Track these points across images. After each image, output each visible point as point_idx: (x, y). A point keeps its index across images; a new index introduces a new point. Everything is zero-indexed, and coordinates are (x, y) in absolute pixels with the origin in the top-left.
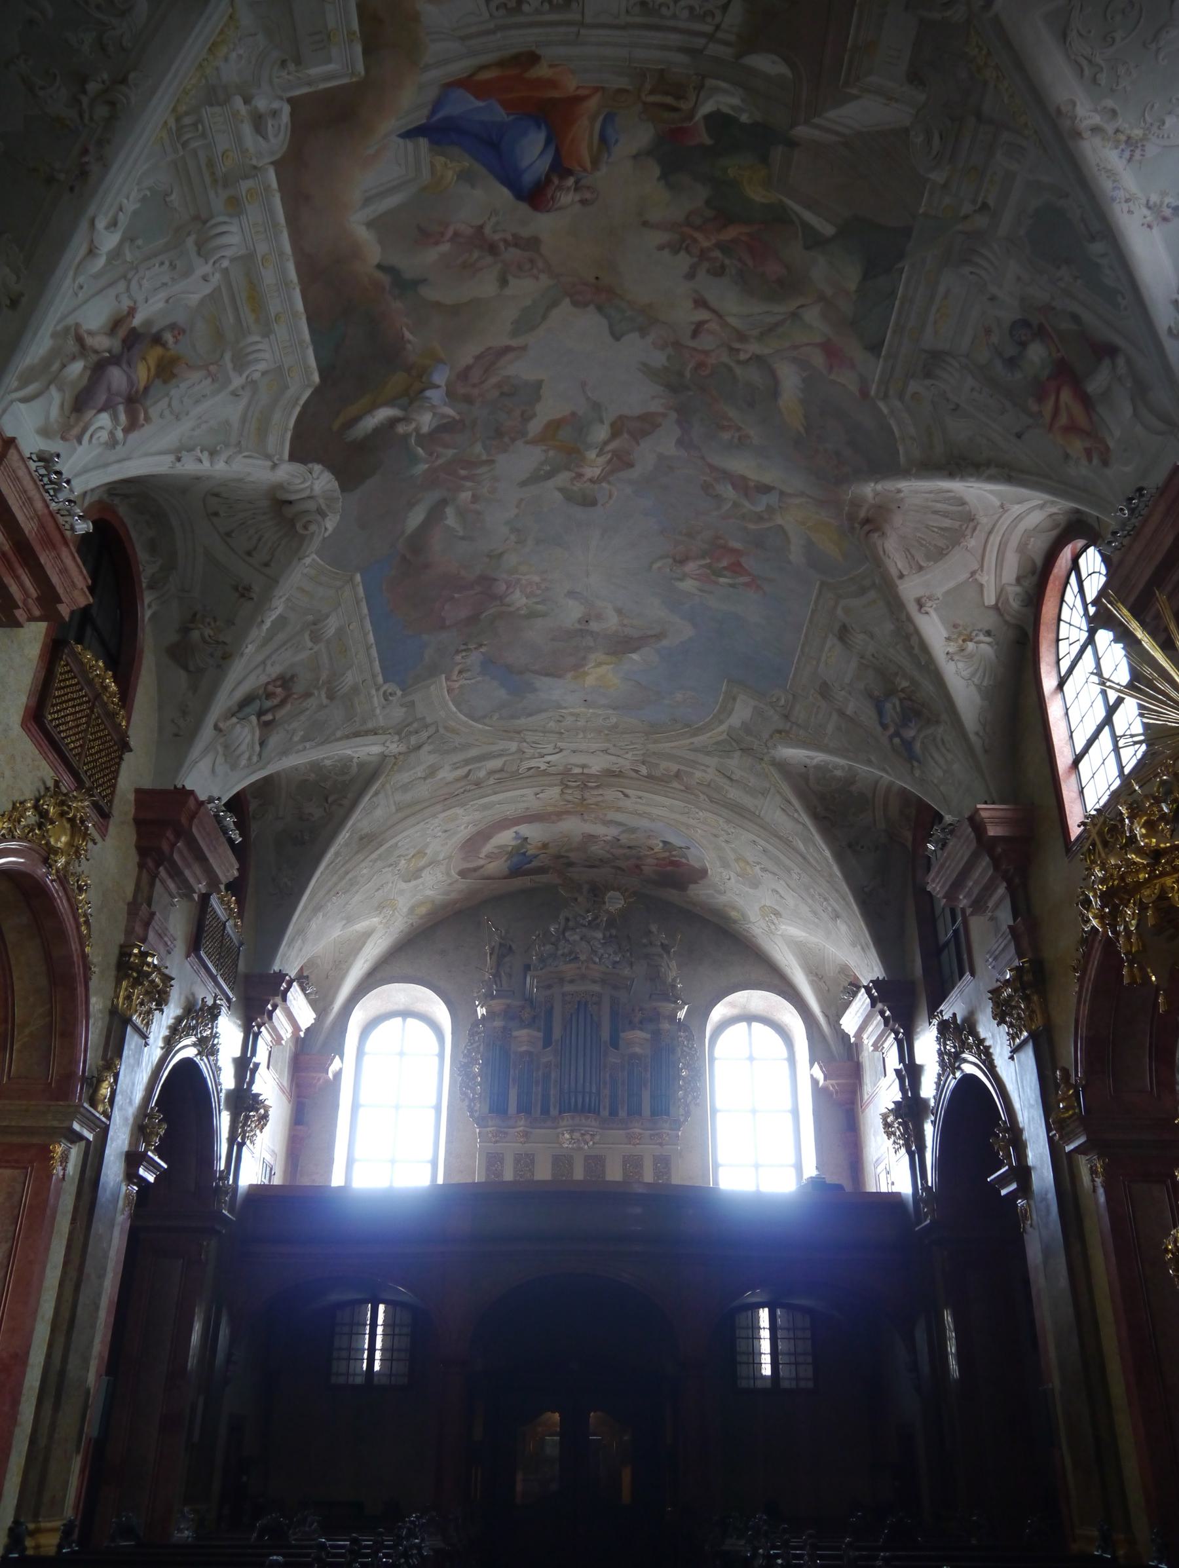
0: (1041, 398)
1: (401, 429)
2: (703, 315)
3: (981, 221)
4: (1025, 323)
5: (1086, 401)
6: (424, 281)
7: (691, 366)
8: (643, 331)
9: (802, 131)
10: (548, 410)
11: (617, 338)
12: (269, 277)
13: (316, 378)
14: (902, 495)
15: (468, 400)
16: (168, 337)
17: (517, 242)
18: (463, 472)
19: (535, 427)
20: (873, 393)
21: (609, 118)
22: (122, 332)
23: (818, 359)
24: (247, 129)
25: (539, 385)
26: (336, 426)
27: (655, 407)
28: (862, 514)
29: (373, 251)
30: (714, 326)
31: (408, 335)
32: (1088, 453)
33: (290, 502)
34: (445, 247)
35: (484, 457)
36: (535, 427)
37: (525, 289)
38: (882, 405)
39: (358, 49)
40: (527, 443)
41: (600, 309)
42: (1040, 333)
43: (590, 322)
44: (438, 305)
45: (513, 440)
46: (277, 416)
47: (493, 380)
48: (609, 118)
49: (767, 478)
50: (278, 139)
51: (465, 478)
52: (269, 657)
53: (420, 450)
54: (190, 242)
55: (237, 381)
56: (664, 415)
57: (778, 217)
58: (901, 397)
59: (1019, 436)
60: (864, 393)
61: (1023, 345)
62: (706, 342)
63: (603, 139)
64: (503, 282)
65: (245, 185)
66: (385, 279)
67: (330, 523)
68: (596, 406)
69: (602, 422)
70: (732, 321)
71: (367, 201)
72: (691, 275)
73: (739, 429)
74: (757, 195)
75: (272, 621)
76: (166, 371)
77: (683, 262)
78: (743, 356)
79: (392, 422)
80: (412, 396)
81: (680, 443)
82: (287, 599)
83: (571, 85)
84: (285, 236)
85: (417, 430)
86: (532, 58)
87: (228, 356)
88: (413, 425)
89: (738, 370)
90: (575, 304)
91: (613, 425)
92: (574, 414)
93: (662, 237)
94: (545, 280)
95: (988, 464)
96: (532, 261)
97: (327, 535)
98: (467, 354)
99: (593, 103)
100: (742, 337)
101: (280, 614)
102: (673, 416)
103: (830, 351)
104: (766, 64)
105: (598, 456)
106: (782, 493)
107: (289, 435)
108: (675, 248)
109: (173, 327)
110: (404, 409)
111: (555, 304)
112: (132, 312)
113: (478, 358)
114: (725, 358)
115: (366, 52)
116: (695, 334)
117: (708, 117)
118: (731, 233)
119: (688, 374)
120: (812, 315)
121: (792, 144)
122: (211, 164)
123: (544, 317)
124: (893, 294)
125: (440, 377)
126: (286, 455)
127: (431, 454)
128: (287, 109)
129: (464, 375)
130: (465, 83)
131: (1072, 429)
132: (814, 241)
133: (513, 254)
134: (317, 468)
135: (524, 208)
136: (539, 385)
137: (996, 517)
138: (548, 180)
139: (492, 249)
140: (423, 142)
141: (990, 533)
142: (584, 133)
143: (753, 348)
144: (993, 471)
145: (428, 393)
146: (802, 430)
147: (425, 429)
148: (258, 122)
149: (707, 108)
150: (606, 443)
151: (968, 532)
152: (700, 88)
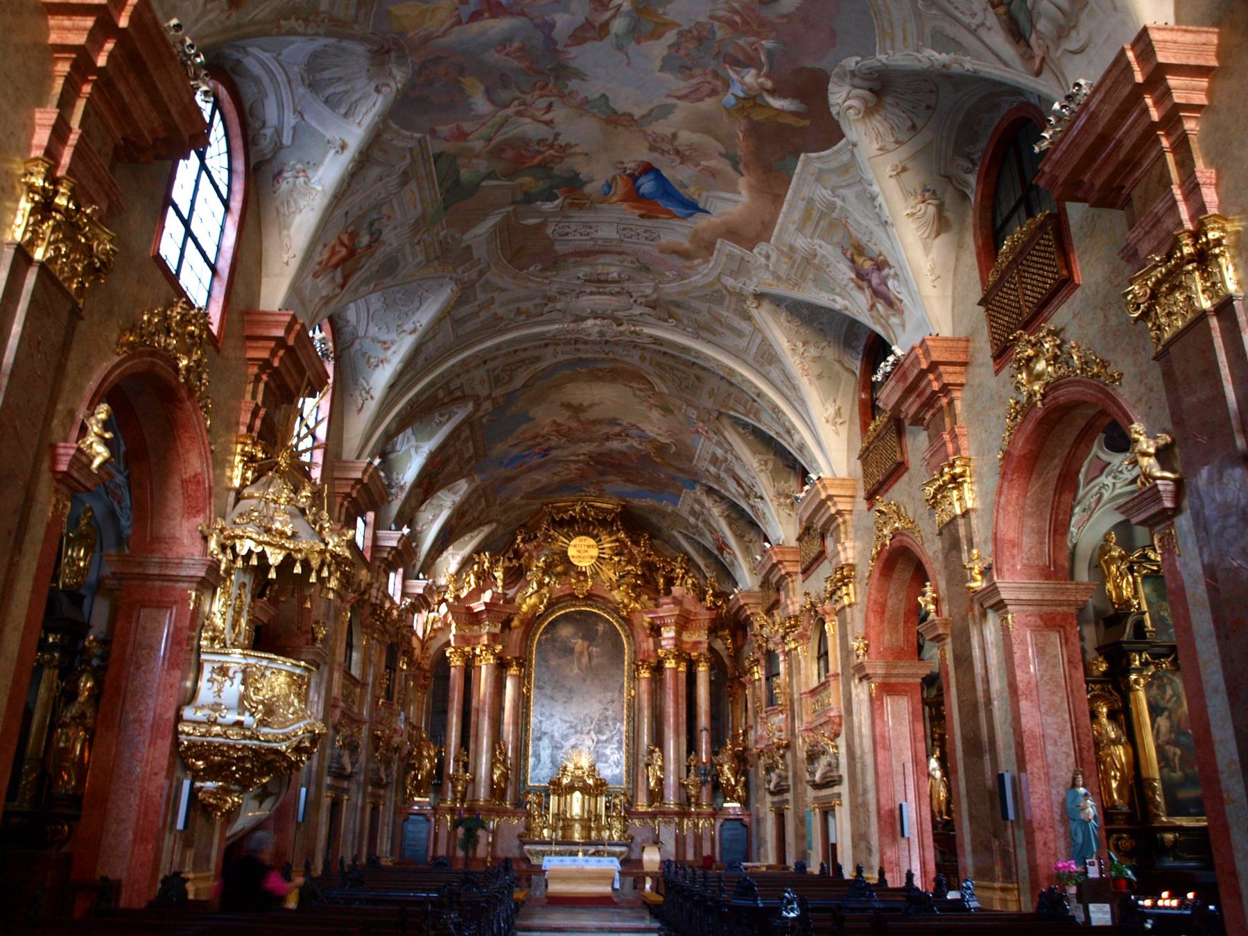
0: (351, 234)
1: (769, 84)
2: (548, 117)
3: (416, 240)
4: (377, 240)
5: (336, 266)
6: (721, 154)
7: (550, 86)
8: (586, 101)
9: (511, 209)
10: (658, 49)
11: (603, 96)
12: (797, 215)
13: (802, 156)
14: (373, 85)
15: (716, 74)
16: (849, 254)
17: (663, 152)
18: (737, 19)
19: (671, 36)
20: (428, 137)
21: (606, 194)
22: (861, 283)
23: (467, 127)
24: (773, 258)
25: (662, 69)
26: (807, 123)
27: (574, 51)
28: (393, 55)
29: (743, 182)
30: (538, 113)
31: (741, 135)
32: (320, 263)
33: (871, 90)
34: (704, 163)
35: (717, 24)
36: (671, 36)
37: (662, 128)
38: (417, 135)
39: (718, 246)
40: (680, 26)
41: (615, 112)
42: (369, 246)
43: (621, 106)
44: (718, 139)
45: (690, 31)
46: (834, 164)
47: (694, 81)
48: (606, 194)
49: (476, 27)
50: (761, 247)
51: (736, 12)
52: (967, 27)
53: (763, 59)
54: (816, 261)
55: (839, 203)
56: (566, 46)
57: (510, 175)
58: (411, 150)
59: (347, 213)
60: (433, 132)
61: (371, 235)
62: (542, 103)
63: (610, 187)
64: (674, 136)
65: (785, 249)
66: (741, 167)
67: (851, 63)
68: (620, 48)
69: (616, 35)
70: (528, 120)
71: (736, 202)
72: (557, 135)
73: (507, 54)
74: (526, 180)
75: (940, 53)
76: (860, 249)
77: (563, 140)
78: (516, 103)
79: (772, 93)
80: (751, 101)
81: (552, 26)
82: (918, 51)
83: (625, 205)
84: (780, 220)
85: (758, 75)
86: (642, 216)
87: (834, 215)
88: (761, 80)
89: (518, 94)
90: (631, 115)
91: (608, 33)
92: (638, 42)
93: (578, 149)
94: (649, 130)
95: (349, 185)
96: (655, 141)
97: (859, 59)
98: (708, 104)
99: (615, 199)
100: (520, 114)
101: (933, 48)
102: (559, 47)
103: (462, 135)
104: (532, 221)
105: (621, 5)
106: (459, 23)
107: (835, 148)
108: (568, 146)
109: (845, 254)
110: (760, 95)
111: (644, 117)
112: (852, 280)
113: (701, 99)
114: (528, 98)
115: (714, 244)
116: (550, 106)
117: (557, 198)
118: (536, 161)
119: (552, 79)
120: (477, 144)
121: (513, 203)
122: (792, 267)
123: (652, 110)
124: (440, 185)
125: (729, 99)
126: (843, 141)
127: (756, 49)
128: (755, 251)
129: (714, 92)
130: (675, 216)
131: (333, 253)
132: (491, 175)
133: (666, 147)
134: (834, 111)
135: (656, 165)
136: (662, 69)
137: (297, 99)
138: (641, 174)
139: (677, 152)
140: (701, 206)
141: (289, 82)
142: (620, 189)
143: (510, 111)
144: (345, 185)
145: (741, 95)
146: (462, 79)
147: (753, 71)
148: (768, 257)
149: (557, 202)
150: (614, 17)
151: (305, 76)
152: (562, 208)
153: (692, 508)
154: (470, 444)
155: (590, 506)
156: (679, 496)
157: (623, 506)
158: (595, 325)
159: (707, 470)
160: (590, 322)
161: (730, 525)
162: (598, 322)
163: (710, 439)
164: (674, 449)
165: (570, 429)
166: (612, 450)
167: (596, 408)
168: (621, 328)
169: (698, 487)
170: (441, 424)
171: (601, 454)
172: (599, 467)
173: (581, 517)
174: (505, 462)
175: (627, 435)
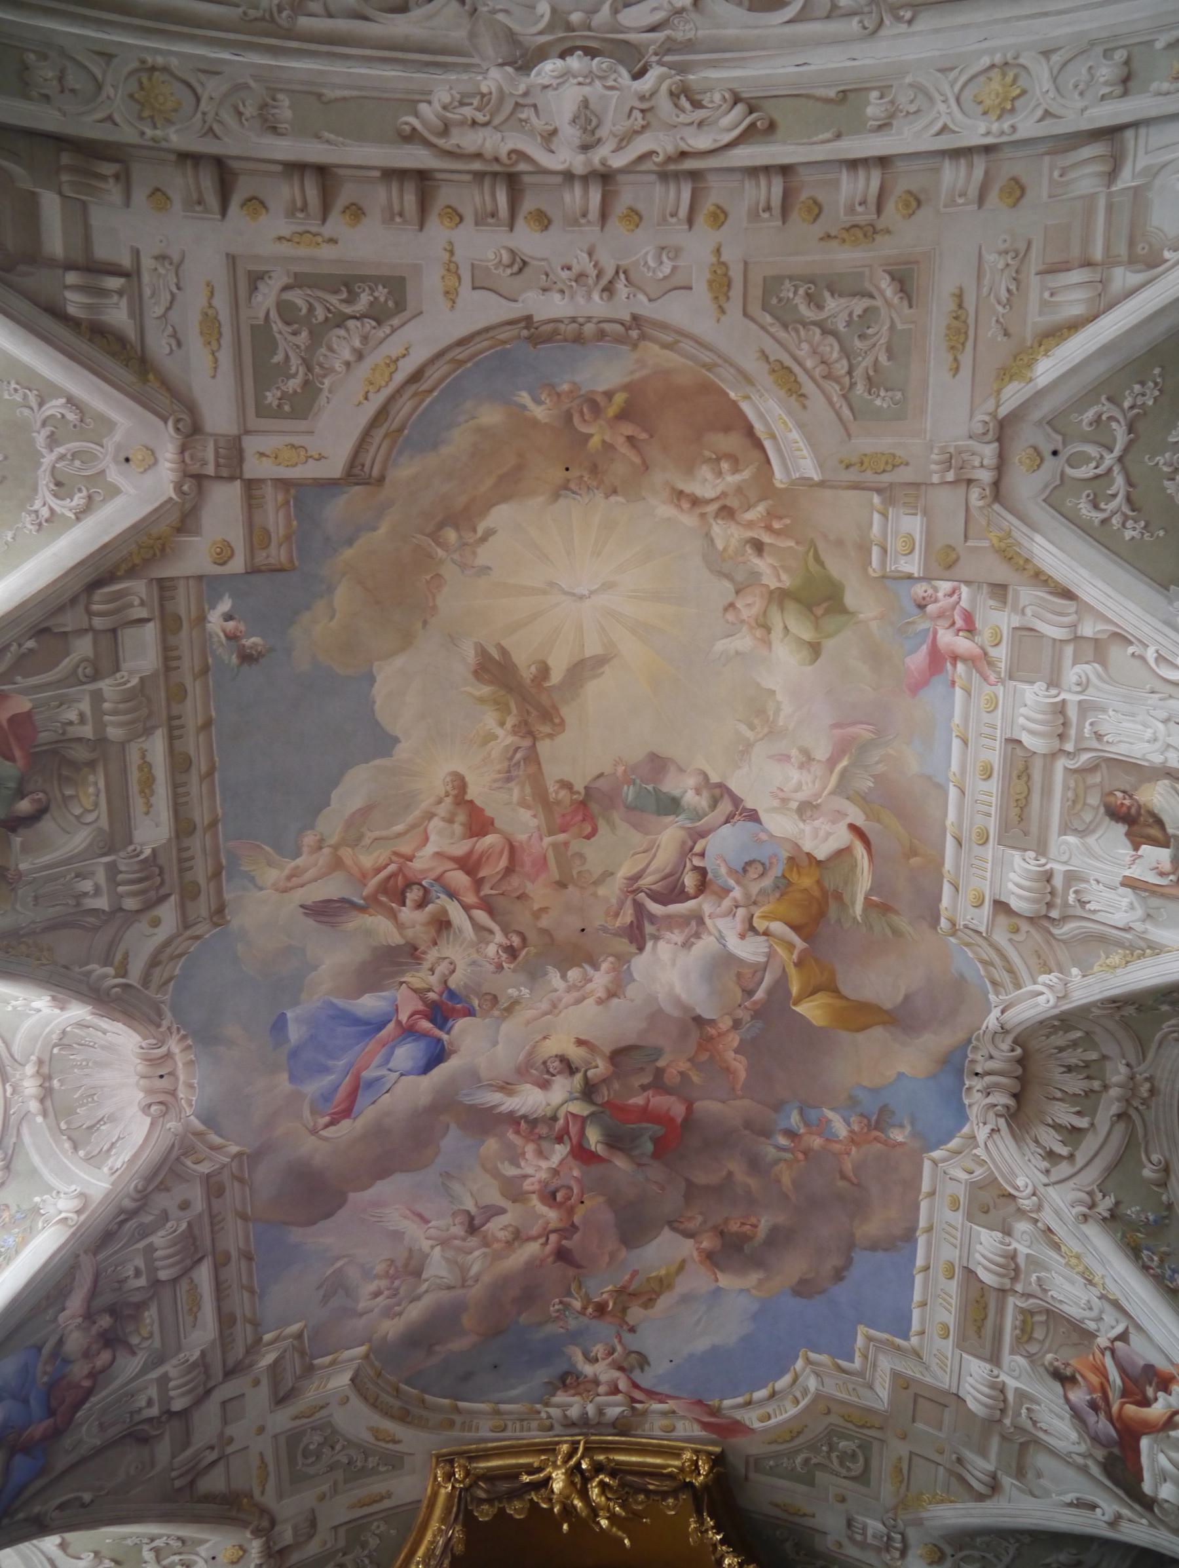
153: (969, 1273)
154: (157, 746)
155: (598, 1468)
156: (909, 1236)
157: (718, 1461)
158: (566, 74)
159: (1001, 906)
160: (550, 67)
161: (1134, 1251)
162: (575, 62)
163: (981, 662)
164: (864, 882)
165: (513, 850)
166: (656, 1016)
167: (592, 688)
168: (646, 84)
169: (975, 1102)
170: (52, 524)
171: (618, 1056)
172: (621, 1163)
173: (568, 1511)
174: (295, 1033)
175: (703, 885)
